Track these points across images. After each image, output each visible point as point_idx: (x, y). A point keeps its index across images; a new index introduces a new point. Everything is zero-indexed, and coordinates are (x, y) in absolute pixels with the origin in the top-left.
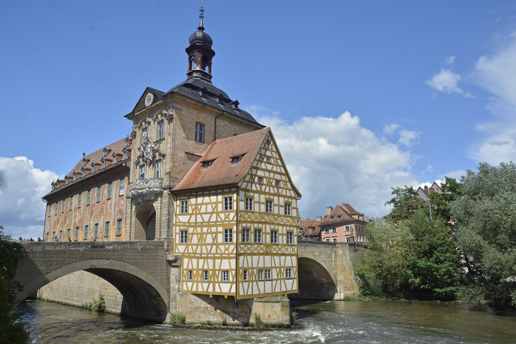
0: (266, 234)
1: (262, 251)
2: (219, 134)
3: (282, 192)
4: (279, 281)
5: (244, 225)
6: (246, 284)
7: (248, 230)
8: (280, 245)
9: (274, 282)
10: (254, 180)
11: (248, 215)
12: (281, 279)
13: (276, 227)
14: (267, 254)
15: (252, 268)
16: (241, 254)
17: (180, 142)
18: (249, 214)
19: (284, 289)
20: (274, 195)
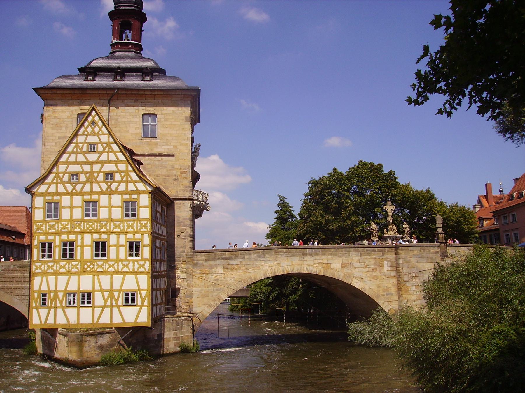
0: (83, 246)
1: (75, 270)
2: (117, 120)
3: (117, 188)
4: (107, 310)
5: (43, 238)
6: (43, 311)
7: (50, 245)
8: (112, 260)
9: (98, 311)
10: (61, 179)
11: (50, 225)
12: (112, 306)
13: (104, 237)
14: (84, 272)
15: (56, 291)
16: (38, 274)
17: (54, 144)
18: (52, 223)
19: (117, 320)
20: (103, 193)
